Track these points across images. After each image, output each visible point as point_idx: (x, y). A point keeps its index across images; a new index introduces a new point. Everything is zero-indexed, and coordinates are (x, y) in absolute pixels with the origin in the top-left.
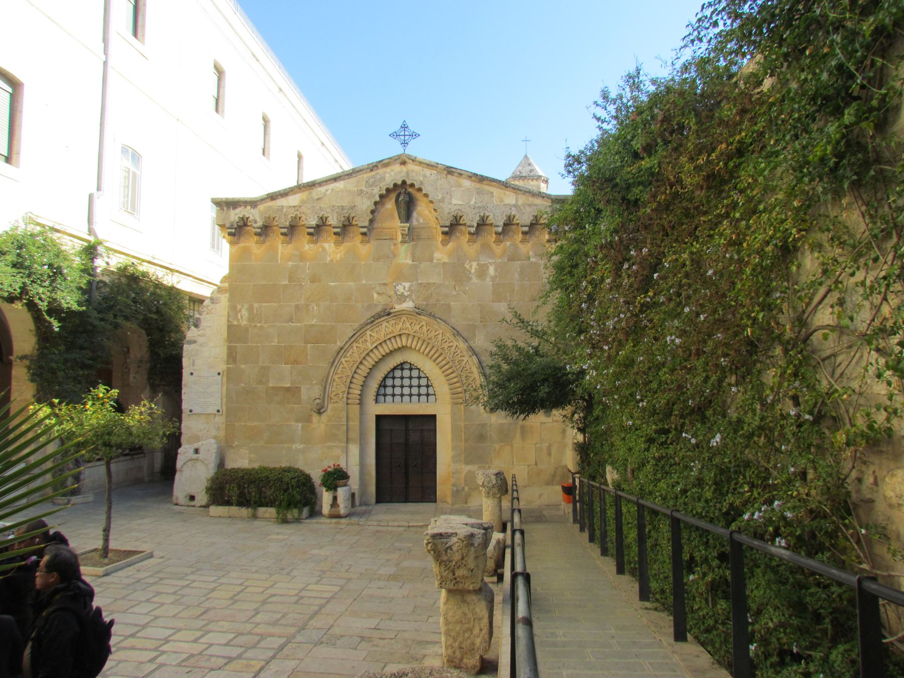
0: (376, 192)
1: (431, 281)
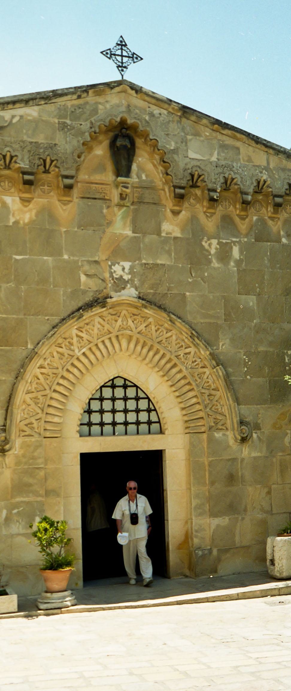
0: (85, 126)
1: (159, 262)
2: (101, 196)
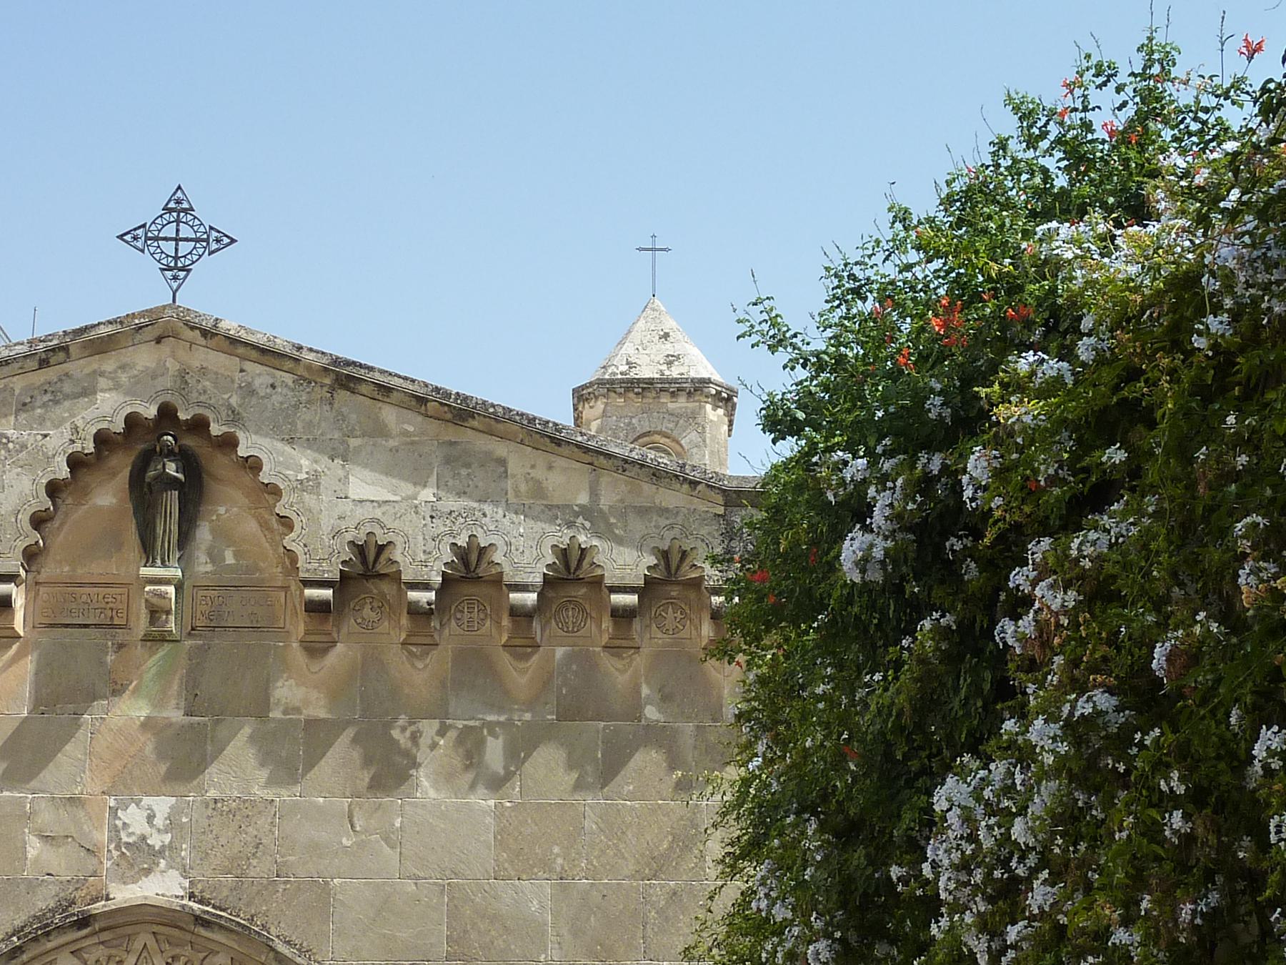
2: (103, 619)
